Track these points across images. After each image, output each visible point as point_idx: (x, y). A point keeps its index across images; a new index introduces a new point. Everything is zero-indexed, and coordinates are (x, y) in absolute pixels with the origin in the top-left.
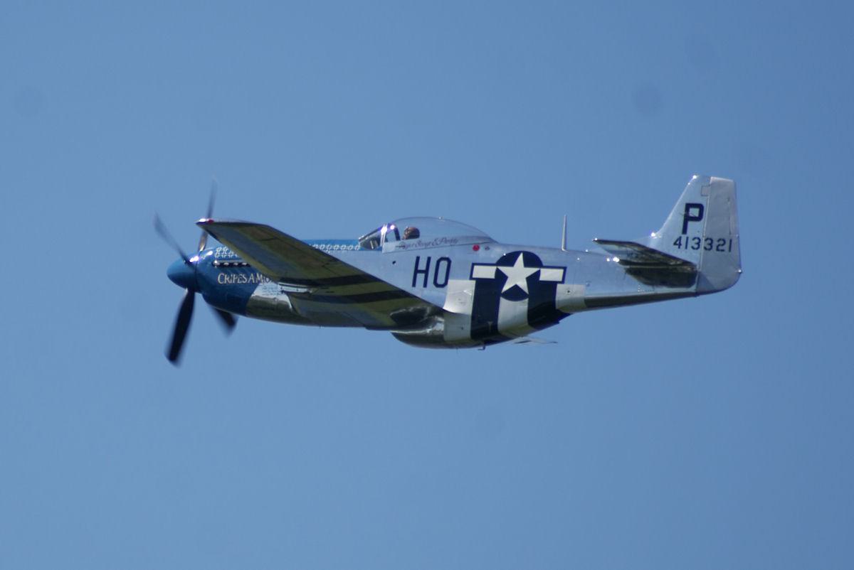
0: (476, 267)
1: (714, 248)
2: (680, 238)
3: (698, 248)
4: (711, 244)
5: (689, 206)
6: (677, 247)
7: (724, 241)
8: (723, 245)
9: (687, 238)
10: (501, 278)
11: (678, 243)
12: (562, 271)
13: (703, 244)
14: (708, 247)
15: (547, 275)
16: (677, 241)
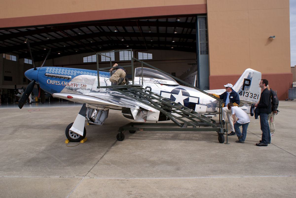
0: (162, 93)
1: (253, 97)
2: (242, 91)
3: (247, 97)
4: (252, 96)
5: (245, 80)
6: (240, 95)
7: (256, 94)
8: (256, 96)
9: (244, 92)
10: (173, 99)
12: (198, 99)
13: (250, 95)
14: (251, 97)
15: (191, 100)
16: (240, 93)
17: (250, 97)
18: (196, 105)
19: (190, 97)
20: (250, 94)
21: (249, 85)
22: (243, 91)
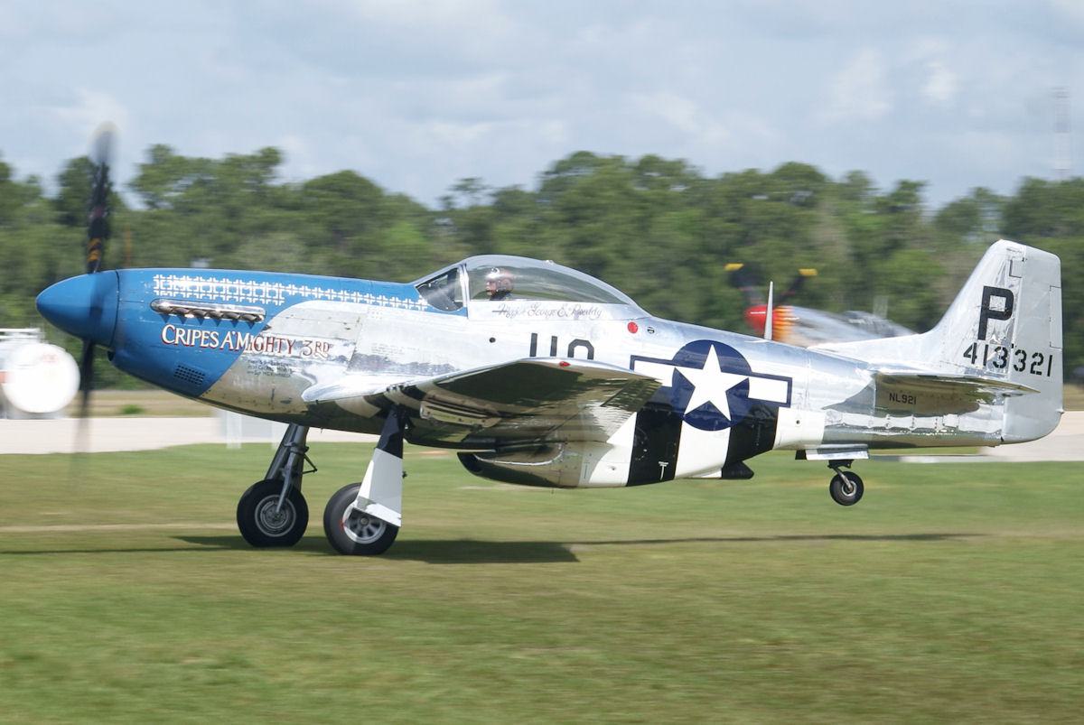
3: (1002, 367)
4: (1023, 361)
5: (989, 292)
6: (970, 359)
8: (1039, 364)
9: (987, 346)
10: (683, 387)
11: (971, 353)
12: (786, 383)
13: (1013, 359)
14: (1020, 366)
15: (760, 390)
17: (1015, 366)
18: (780, 408)
19: (751, 379)
20: (1012, 353)
21: (1006, 315)
22: (981, 344)
